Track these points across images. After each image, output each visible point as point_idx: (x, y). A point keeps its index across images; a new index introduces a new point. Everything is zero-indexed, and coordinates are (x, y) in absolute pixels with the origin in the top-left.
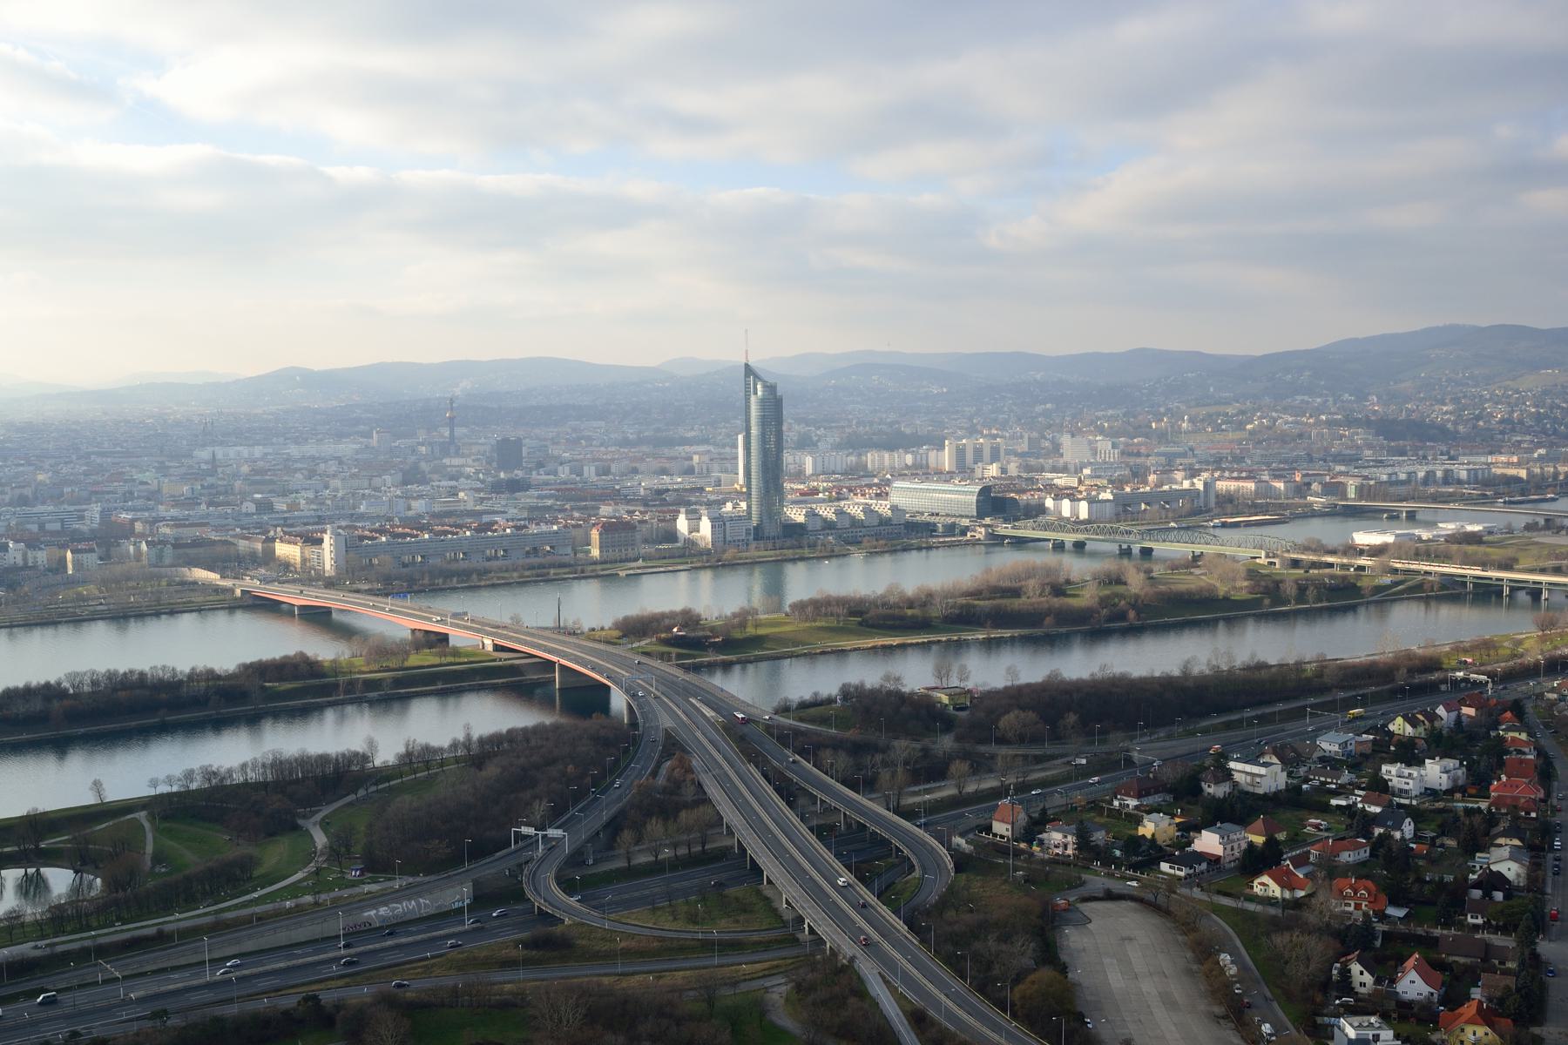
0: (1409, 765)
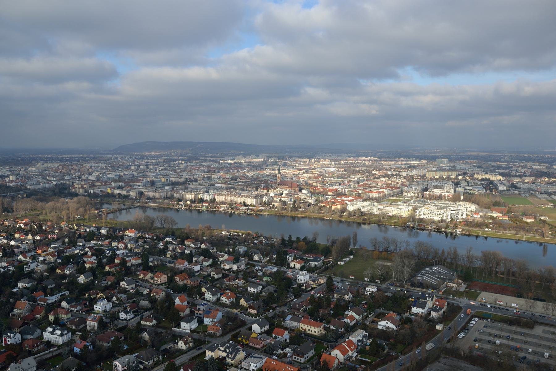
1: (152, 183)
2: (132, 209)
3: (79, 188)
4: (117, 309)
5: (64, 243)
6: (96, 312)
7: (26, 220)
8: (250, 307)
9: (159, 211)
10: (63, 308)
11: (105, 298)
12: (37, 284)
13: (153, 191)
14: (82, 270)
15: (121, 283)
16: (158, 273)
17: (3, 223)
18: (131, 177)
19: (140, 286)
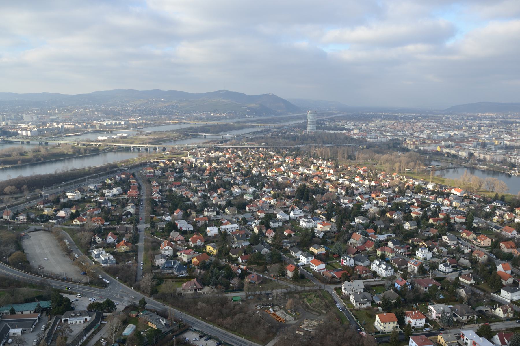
0: (110, 189)
1: (484, 145)
2: (459, 169)
3: (411, 144)
4: (436, 260)
5: (394, 192)
6: (417, 257)
7: (365, 168)
9: (488, 174)
10: (389, 247)
11: (427, 248)
12: (370, 222)
13: (484, 154)
14: (408, 218)
15: (443, 237)
16: (482, 235)
17: (347, 168)
18: (462, 138)
19: (461, 244)
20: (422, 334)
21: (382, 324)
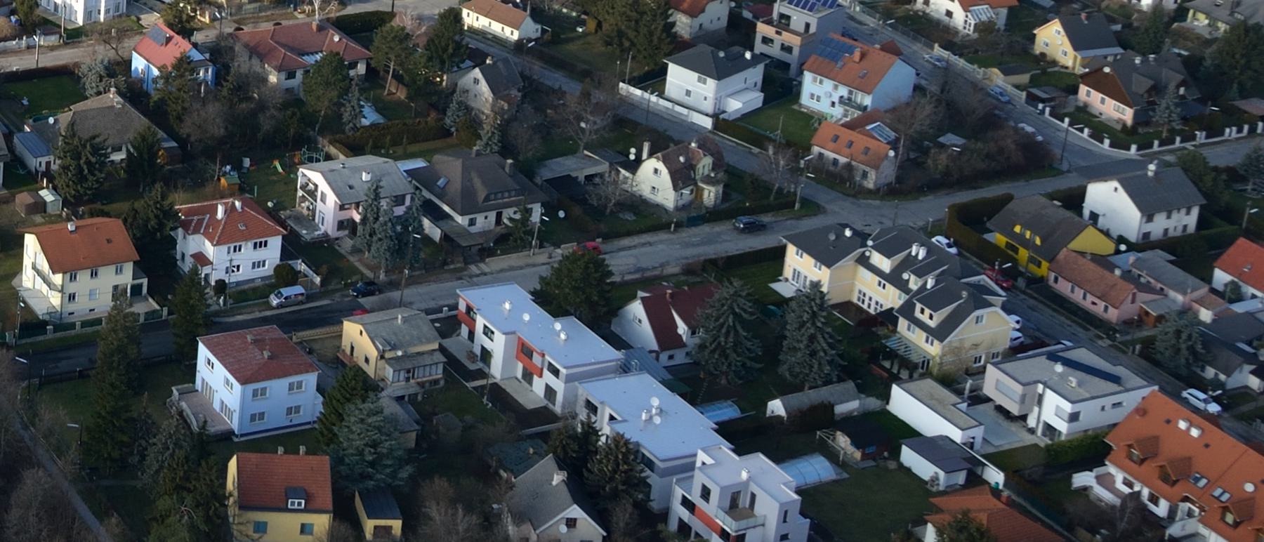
8: (1095, 79)
20: (265, 321)
21: (58, 279)
